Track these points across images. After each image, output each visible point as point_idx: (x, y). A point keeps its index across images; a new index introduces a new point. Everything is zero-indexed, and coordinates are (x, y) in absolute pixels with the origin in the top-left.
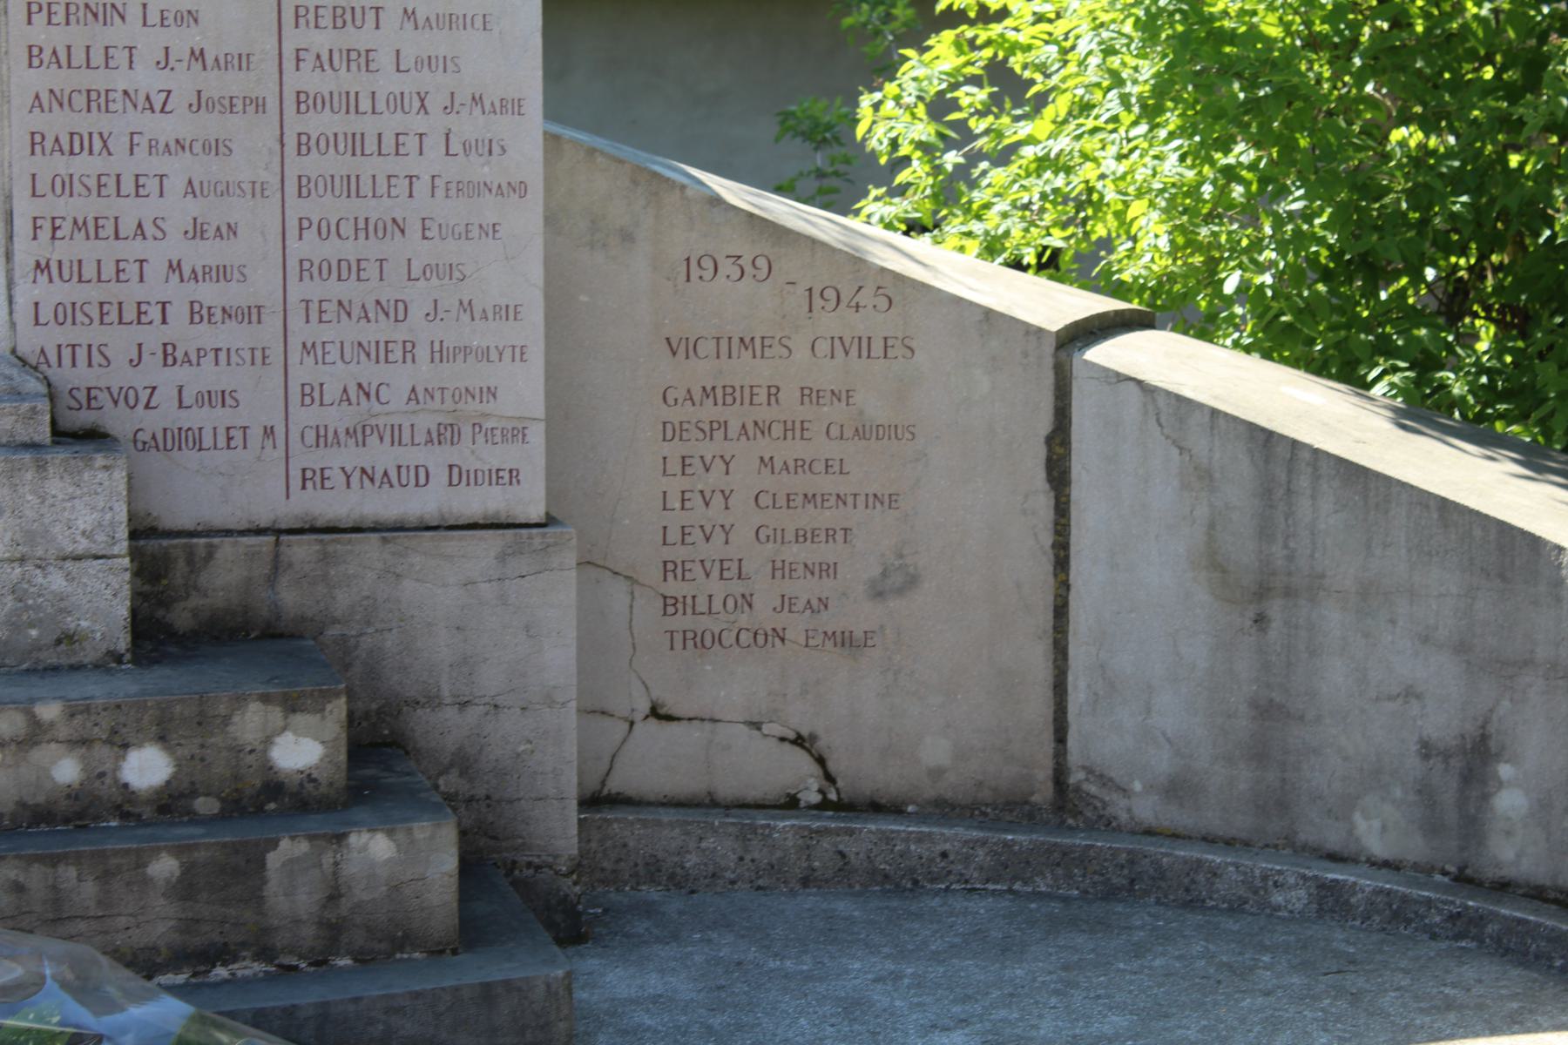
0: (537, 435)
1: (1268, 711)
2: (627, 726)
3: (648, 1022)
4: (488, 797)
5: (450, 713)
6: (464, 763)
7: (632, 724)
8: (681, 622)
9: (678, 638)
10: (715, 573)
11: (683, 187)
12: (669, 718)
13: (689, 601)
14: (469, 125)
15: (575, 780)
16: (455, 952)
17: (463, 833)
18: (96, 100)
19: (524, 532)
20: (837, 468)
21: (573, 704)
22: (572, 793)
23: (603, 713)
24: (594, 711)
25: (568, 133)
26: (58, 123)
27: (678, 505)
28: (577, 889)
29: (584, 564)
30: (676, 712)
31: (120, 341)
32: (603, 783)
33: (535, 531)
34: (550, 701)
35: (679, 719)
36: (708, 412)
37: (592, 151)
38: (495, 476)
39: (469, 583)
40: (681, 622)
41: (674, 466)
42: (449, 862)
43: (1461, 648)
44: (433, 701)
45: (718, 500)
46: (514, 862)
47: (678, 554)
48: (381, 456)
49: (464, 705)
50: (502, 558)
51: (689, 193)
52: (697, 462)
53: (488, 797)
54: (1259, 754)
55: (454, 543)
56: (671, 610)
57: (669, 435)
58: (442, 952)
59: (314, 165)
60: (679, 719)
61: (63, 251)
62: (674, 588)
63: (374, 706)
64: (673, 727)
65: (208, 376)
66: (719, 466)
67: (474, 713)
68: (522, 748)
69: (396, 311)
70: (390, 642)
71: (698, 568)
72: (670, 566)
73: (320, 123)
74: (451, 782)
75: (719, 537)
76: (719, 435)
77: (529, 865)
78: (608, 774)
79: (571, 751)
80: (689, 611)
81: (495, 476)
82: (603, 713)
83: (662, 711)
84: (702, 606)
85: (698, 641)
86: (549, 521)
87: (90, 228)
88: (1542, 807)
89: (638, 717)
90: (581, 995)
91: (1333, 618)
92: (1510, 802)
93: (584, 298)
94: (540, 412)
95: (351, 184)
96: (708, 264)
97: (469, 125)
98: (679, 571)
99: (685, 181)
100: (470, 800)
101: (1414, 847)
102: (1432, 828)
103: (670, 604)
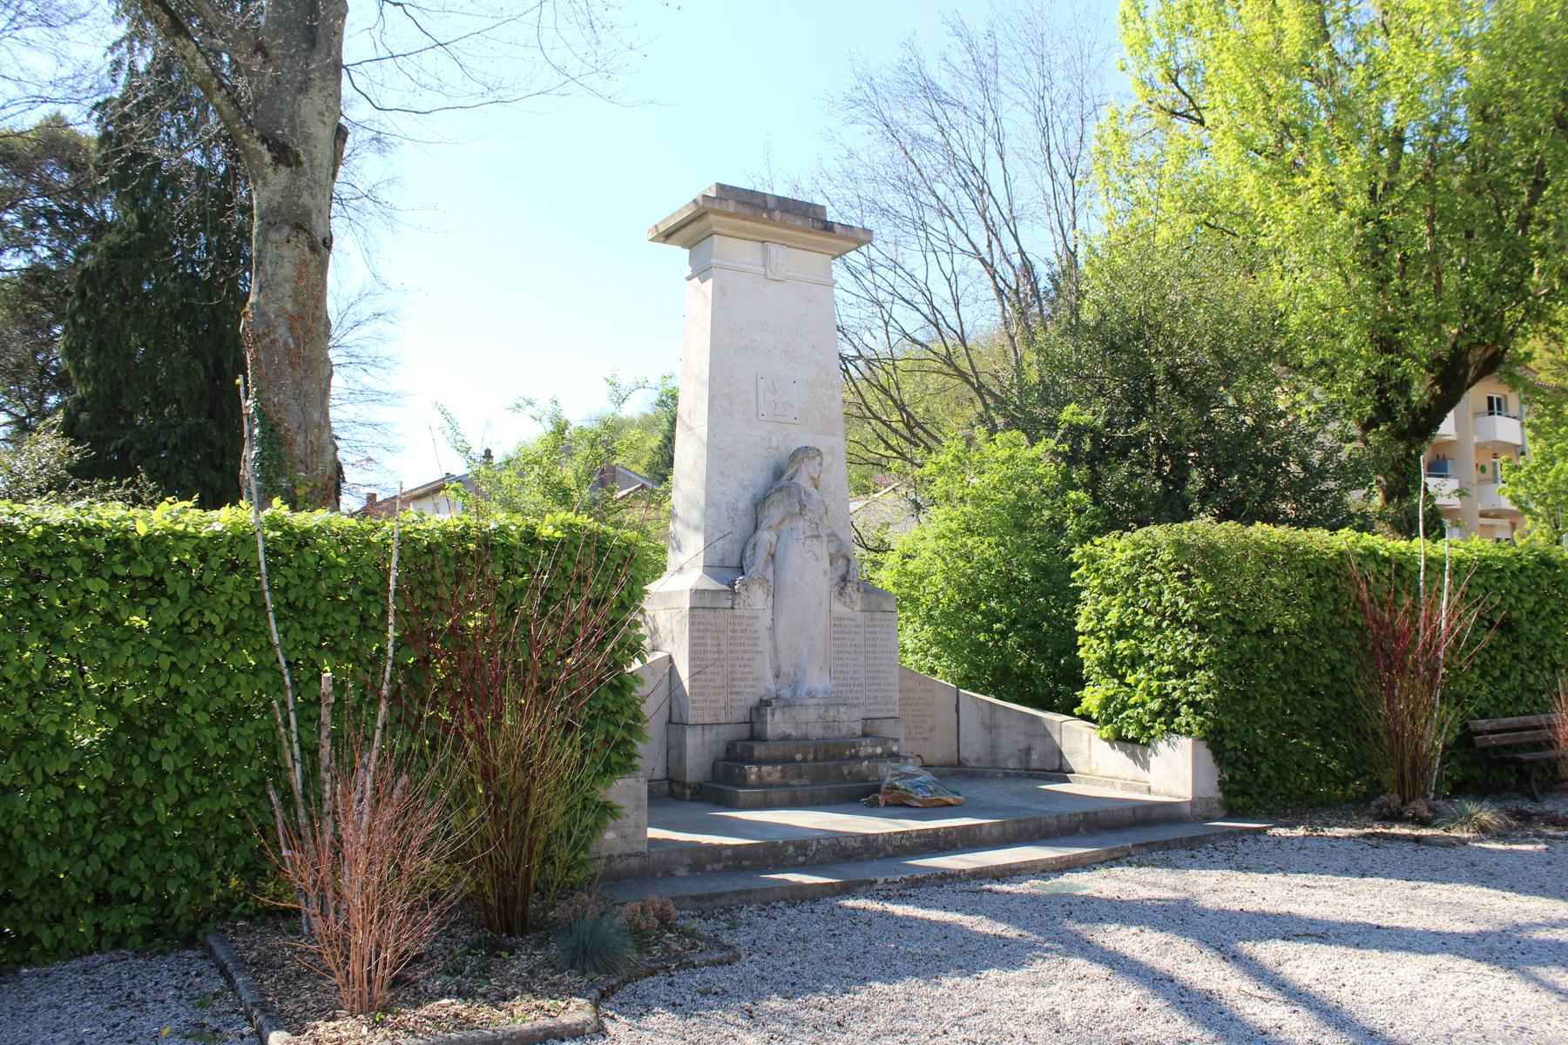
1: (993, 747)
14: (889, 655)
18: (842, 652)
26: (837, 656)
31: (844, 689)
43: (1025, 734)
48: (877, 707)
54: (991, 754)
59: (870, 662)
61: (838, 675)
65: (855, 695)
69: (879, 684)
73: (871, 655)
87: (840, 672)
88: (1040, 757)
91: (1003, 731)
92: (1034, 756)
95: (874, 665)
97: (889, 655)
101: (1018, 766)
102: (1020, 762)
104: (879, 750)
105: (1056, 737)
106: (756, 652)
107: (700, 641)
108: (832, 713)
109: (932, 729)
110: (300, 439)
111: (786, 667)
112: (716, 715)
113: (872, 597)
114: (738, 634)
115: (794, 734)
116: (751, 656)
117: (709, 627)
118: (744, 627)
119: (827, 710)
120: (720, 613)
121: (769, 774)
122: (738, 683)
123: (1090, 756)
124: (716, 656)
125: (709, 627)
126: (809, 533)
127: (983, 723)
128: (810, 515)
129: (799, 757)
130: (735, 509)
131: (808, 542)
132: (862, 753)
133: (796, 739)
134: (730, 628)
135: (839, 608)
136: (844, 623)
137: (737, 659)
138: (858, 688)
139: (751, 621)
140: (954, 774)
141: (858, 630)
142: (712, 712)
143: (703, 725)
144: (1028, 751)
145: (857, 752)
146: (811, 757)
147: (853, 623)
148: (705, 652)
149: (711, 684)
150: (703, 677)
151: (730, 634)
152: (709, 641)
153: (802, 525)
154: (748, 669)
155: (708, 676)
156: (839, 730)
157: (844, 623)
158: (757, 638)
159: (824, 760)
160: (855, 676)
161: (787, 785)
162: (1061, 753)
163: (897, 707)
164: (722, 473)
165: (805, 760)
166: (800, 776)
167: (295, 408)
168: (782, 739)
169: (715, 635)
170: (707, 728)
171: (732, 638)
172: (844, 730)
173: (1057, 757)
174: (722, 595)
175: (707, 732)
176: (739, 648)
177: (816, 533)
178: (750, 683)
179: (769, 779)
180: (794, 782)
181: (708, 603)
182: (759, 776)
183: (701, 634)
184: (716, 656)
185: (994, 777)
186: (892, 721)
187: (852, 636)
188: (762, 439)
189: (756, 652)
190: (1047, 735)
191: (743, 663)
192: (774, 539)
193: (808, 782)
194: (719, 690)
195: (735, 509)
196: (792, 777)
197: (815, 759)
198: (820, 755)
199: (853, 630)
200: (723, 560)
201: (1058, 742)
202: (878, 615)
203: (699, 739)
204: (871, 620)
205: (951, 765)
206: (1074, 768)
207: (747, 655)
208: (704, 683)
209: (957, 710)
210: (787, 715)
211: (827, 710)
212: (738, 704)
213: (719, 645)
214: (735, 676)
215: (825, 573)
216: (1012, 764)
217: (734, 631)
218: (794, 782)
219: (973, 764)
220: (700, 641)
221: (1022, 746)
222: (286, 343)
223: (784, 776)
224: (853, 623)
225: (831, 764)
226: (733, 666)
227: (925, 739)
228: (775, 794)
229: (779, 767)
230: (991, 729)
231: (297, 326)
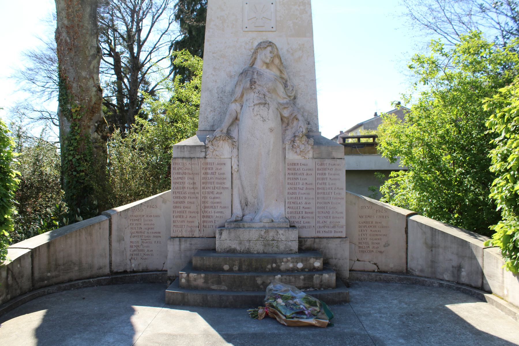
0: (345, 227)
1: (433, 262)
5: (334, 260)
6: (336, 266)
8: (361, 249)
12: (359, 261)
14: (337, 191)
17: (336, 274)
18: (295, 189)
22: (348, 270)
24: (350, 260)
25: (348, 192)
26: (291, 191)
31: (297, 216)
34: (346, 259)
36: (364, 224)
40: (361, 249)
41: (360, 231)
43: (457, 254)
44: (332, 258)
45: (365, 235)
47: (361, 241)
48: (327, 229)
49: (336, 259)
50: (340, 242)
55: (335, 240)
59: (319, 196)
61: (291, 205)
62: (360, 245)
65: (307, 220)
67: (337, 260)
69: (328, 213)
70: (327, 251)
73: (320, 191)
74: (334, 268)
79: (348, 265)
84: (363, 247)
85: (363, 252)
86: (346, 237)
91: (441, 250)
92: (464, 274)
95: (323, 198)
97: (337, 191)
100: (336, 270)
101: (451, 279)
102: (454, 276)
104: (300, 265)
105: (480, 261)
106: (223, 188)
107: (180, 180)
108: (272, 234)
109: (387, 245)
110: (75, 85)
111: (250, 199)
112: (192, 231)
113: (323, 148)
114: (209, 176)
115: (238, 248)
116: (222, 191)
118: (214, 171)
119: (267, 232)
121: (195, 280)
122: (210, 210)
123: (503, 282)
124: (192, 191)
125: (187, 171)
126: (256, 102)
127: (426, 243)
129: (226, 267)
130: (223, 92)
131: (256, 108)
132: (283, 266)
133: (240, 253)
134: (203, 171)
135: (291, 156)
136: (297, 167)
138: (309, 215)
139: (219, 167)
140: (400, 280)
141: (309, 172)
142: (189, 229)
144: (459, 268)
145: (278, 266)
146: (236, 268)
148: (184, 188)
149: (188, 210)
150: (182, 205)
151: (203, 176)
152: (186, 181)
153: (252, 97)
154: (217, 200)
155: (186, 205)
156: (278, 247)
157: (297, 167)
158: (225, 179)
159: (248, 271)
160: (307, 206)
162: (483, 274)
163: (344, 230)
164: (214, 68)
165: (231, 270)
166: (219, 283)
167: (72, 70)
168: (228, 252)
169: (191, 176)
170: (183, 240)
171: (204, 178)
172: (282, 247)
173: (480, 277)
174: (198, 149)
175: (183, 243)
176: (209, 185)
177: (263, 101)
178: (219, 210)
179: (194, 283)
180: (214, 287)
181: (187, 155)
182: (188, 280)
183: (180, 176)
184: (192, 191)
185: (431, 285)
186: (339, 240)
187: (305, 177)
188: (246, 43)
189: (223, 188)
190: (473, 257)
191: (213, 196)
192: (239, 108)
193: (226, 288)
195: (223, 92)
196: (213, 283)
197: (240, 270)
198: (244, 267)
199: (305, 172)
200: (213, 126)
201: (481, 264)
202: (327, 161)
203: (177, 248)
204: (322, 164)
205: (400, 273)
206: (493, 289)
207: (216, 191)
208: (182, 209)
209: (406, 232)
210: (233, 234)
211: (267, 232)
212: (210, 224)
213: (194, 183)
214: (207, 205)
215: (271, 130)
216: (447, 276)
217: (206, 173)
218: (214, 287)
219: (417, 273)
220: (180, 180)
221: (455, 263)
222: (66, 41)
223: (206, 281)
225: (246, 275)
226: (205, 198)
227: (381, 252)
228: (191, 296)
229: (203, 275)
230: (432, 247)
231: (71, 31)
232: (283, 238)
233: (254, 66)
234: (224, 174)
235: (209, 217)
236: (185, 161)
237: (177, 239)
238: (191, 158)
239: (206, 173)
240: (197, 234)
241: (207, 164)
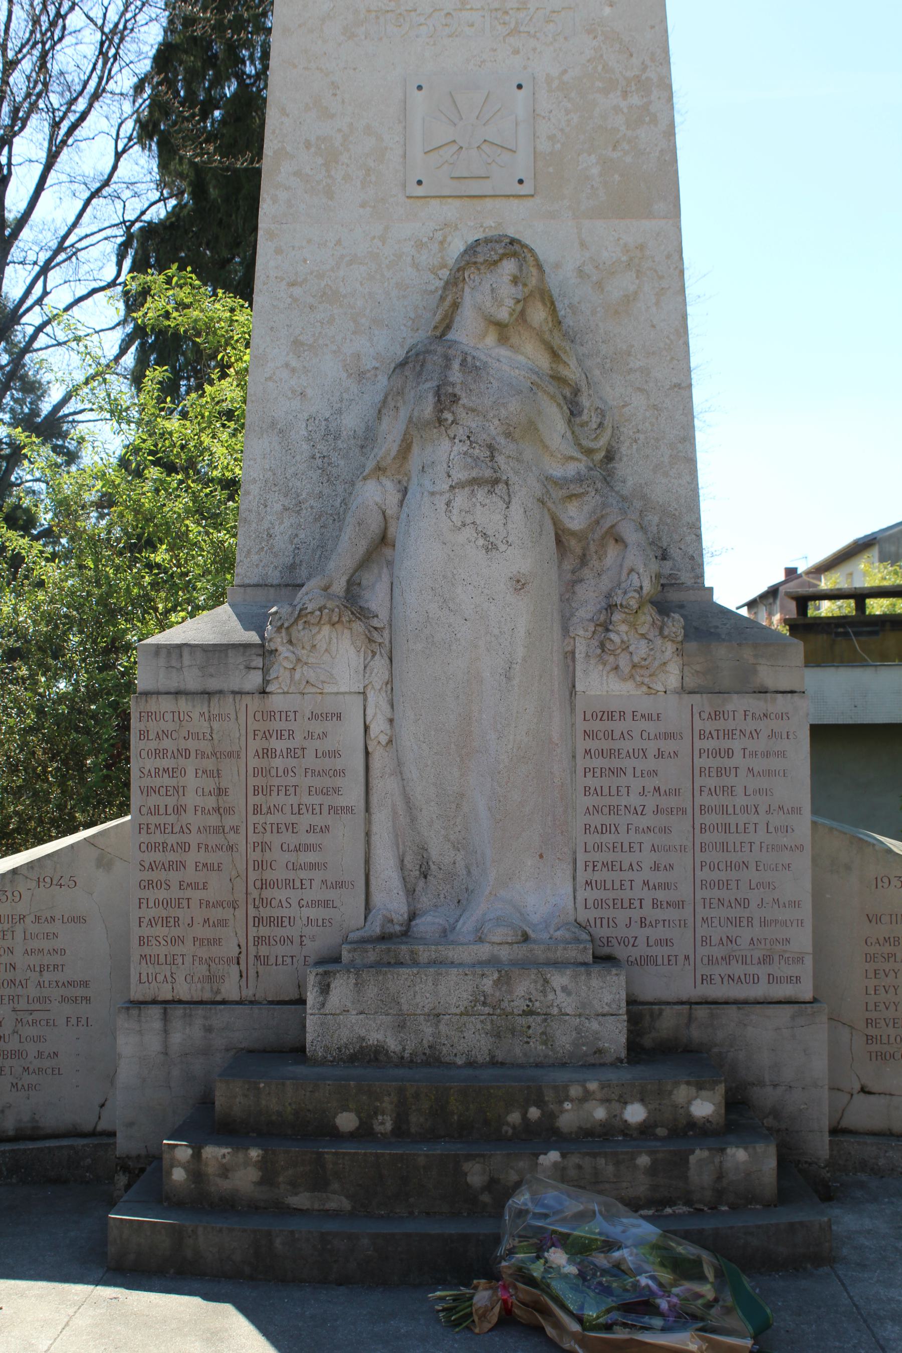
0: (809, 961)
2: (849, 1096)
3: (867, 1243)
4: (787, 1129)
5: (769, 1089)
6: (775, 1113)
7: (852, 1095)
8: (875, 1047)
9: (874, 1055)
10: (891, 1024)
11: (874, 845)
12: (870, 1093)
13: (879, 1038)
15: (827, 1123)
16: (775, 1206)
17: (777, 1146)
18: (613, 810)
19: (803, 1006)
20: (618, 867)
21: (827, 1087)
22: (826, 1129)
23: (838, 1089)
25: (820, 820)
26: (596, 820)
27: (873, 992)
28: (829, 1175)
29: (830, 1019)
30: (873, 1090)
31: (622, 916)
32: (839, 1123)
33: (808, 1005)
35: (874, 1093)
36: (887, 949)
37: (831, 829)
38: (789, 979)
39: (777, 1029)
40: (875, 1047)
41: (871, 974)
42: (771, 1163)
44: (761, 1084)
45: (892, 990)
46: (799, 1161)
47: (874, 1015)
48: (737, 969)
49: (775, 1086)
50: (793, 1018)
51: (877, 848)
52: (882, 972)
53: (787, 1129)
55: (771, 1010)
56: (870, 1042)
57: (868, 960)
58: (769, 1206)
59: (708, 837)
60: (874, 1093)
61: (597, 876)
62: (872, 1031)
63: (734, 1085)
64: (871, 1097)
65: (660, 932)
66: (892, 974)
68: (802, 1107)
69: (744, 903)
71: (883, 1022)
72: (869, 1021)
73: (711, 819)
74: (769, 1121)
75: (892, 1007)
76: (892, 960)
77: (806, 1162)
78: (841, 1118)
79: (826, 1109)
80: (879, 1042)
81: (789, 979)
82: (838, 1089)
83: (866, 1090)
84: (885, 1040)
85: (882, 1057)
86: (815, 1000)
87: (609, 866)
89: (855, 1092)
90: (834, 1228)
93: (828, 896)
94: (810, 949)
95: (724, 847)
96: (886, 880)
98: (874, 1024)
99: (875, 842)
100: (778, 1131)
103: (869, 1039)
104: (635, 1113)
106: (334, 810)
107: (166, 780)
111: (439, 850)
112: (211, 978)
113: (721, 651)
114: (278, 762)
115: (393, 1045)
117: (192, 744)
119: (504, 980)
120: (227, 705)
121: (225, 1171)
122: (281, 894)
124: (213, 820)
125: (192, 744)
126: (460, 475)
128: (471, 422)
129: (347, 1121)
130: (332, 435)
131: (461, 499)
133: (402, 1062)
134: (255, 745)
136: (619, 727)
137: (277, 828)
138: (671, 914)
139: (317, 727)
141: (668, 746)
143: (166, 1004)
145: (550, 1117)
146: (385, 1124)
147: (651, 727)
148: (179, 809)
149: (196, 895)
150: (174, 877)
151: (253, 762)
152: (191, 781)
154: (310, 857)
155: (190, 875)
156: (547, 1039)
157: (619, 727)
159: (430, 1136)
161: (282, 1210)
165: (364, 1133)
168: (353, 1059)
169: (210, 764)
170: (179, 1011)
172: (564, 1040)
177: (488, 473)
178: (315, 893)
180: (300, 1200)
181: (191, 680)
182: (196, 1173)
183: (167, 763)
184: (213, 820)
186: (789, 1010)
187: (651, 763)
189: (334, 810)
191: (291, 839)
192: (393, 498)
193: (346, 1204)
194: (217, 914)
195: (332, 435)
197: (400, 1132)
198: (416, 1120)
199: (652, 747)
200: (292, 567)
202: (737, 703)
203: (154, 1043)
204: (716, 715)
207: (306, 820)
208: (175, 893)
210: (371, 991)
211: (504, 980)
212: (281, 950)
213: (221, 792)
214: (269, 875)
215: (519, 584)
217: (267, 753)
220: (166, 780)
223: (268, 1178)
224: (651, 727)
226: (264, 846)
229: (254, 1153)
232: (568, 1004)
233: (450, 336)
234: (335, 754)
235: (279, 922)
236: (183, 705)
237: (155, 1012)
238: (208, 694)
239: (267, 753)
240: (230, 989)
241: (271, 715)
